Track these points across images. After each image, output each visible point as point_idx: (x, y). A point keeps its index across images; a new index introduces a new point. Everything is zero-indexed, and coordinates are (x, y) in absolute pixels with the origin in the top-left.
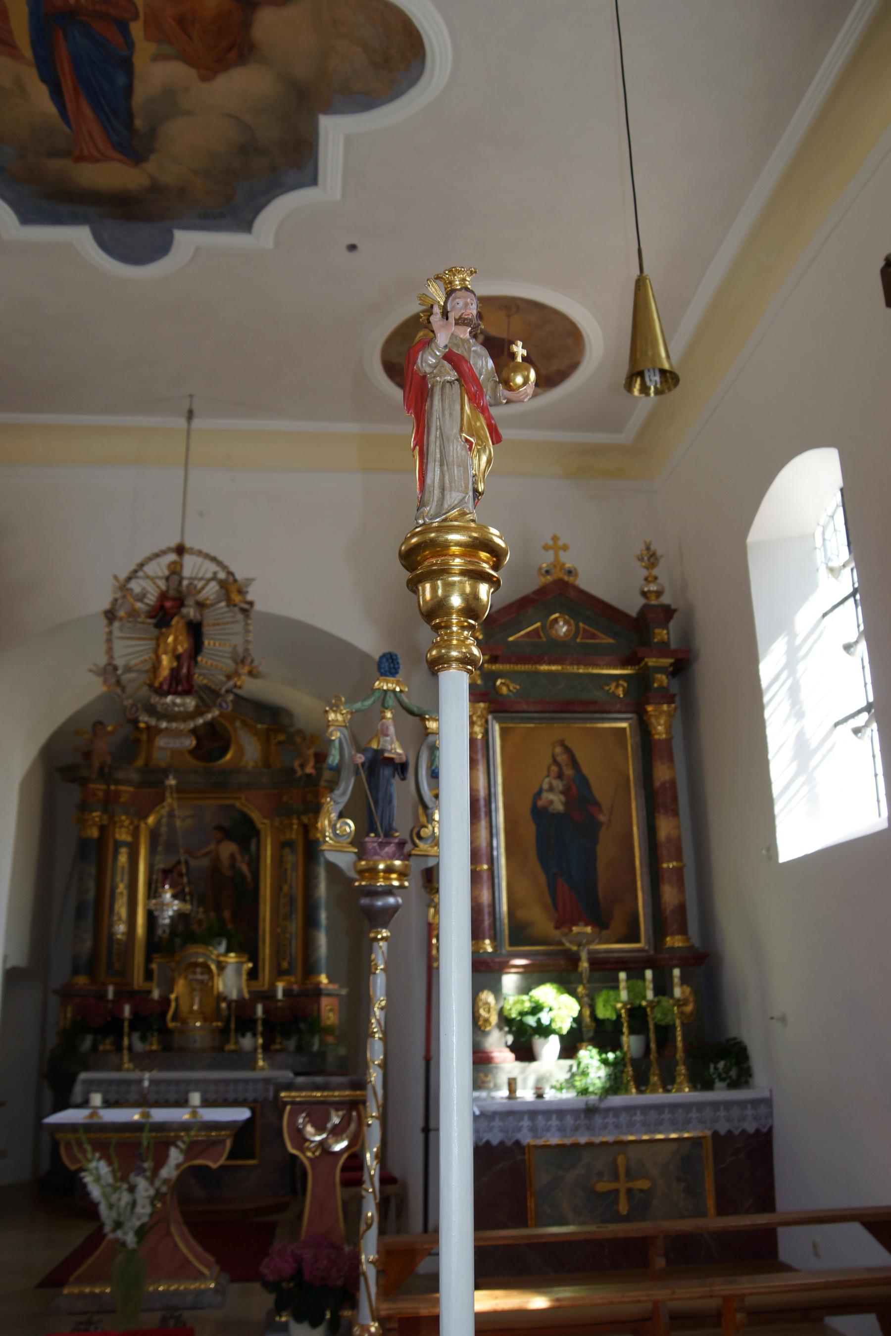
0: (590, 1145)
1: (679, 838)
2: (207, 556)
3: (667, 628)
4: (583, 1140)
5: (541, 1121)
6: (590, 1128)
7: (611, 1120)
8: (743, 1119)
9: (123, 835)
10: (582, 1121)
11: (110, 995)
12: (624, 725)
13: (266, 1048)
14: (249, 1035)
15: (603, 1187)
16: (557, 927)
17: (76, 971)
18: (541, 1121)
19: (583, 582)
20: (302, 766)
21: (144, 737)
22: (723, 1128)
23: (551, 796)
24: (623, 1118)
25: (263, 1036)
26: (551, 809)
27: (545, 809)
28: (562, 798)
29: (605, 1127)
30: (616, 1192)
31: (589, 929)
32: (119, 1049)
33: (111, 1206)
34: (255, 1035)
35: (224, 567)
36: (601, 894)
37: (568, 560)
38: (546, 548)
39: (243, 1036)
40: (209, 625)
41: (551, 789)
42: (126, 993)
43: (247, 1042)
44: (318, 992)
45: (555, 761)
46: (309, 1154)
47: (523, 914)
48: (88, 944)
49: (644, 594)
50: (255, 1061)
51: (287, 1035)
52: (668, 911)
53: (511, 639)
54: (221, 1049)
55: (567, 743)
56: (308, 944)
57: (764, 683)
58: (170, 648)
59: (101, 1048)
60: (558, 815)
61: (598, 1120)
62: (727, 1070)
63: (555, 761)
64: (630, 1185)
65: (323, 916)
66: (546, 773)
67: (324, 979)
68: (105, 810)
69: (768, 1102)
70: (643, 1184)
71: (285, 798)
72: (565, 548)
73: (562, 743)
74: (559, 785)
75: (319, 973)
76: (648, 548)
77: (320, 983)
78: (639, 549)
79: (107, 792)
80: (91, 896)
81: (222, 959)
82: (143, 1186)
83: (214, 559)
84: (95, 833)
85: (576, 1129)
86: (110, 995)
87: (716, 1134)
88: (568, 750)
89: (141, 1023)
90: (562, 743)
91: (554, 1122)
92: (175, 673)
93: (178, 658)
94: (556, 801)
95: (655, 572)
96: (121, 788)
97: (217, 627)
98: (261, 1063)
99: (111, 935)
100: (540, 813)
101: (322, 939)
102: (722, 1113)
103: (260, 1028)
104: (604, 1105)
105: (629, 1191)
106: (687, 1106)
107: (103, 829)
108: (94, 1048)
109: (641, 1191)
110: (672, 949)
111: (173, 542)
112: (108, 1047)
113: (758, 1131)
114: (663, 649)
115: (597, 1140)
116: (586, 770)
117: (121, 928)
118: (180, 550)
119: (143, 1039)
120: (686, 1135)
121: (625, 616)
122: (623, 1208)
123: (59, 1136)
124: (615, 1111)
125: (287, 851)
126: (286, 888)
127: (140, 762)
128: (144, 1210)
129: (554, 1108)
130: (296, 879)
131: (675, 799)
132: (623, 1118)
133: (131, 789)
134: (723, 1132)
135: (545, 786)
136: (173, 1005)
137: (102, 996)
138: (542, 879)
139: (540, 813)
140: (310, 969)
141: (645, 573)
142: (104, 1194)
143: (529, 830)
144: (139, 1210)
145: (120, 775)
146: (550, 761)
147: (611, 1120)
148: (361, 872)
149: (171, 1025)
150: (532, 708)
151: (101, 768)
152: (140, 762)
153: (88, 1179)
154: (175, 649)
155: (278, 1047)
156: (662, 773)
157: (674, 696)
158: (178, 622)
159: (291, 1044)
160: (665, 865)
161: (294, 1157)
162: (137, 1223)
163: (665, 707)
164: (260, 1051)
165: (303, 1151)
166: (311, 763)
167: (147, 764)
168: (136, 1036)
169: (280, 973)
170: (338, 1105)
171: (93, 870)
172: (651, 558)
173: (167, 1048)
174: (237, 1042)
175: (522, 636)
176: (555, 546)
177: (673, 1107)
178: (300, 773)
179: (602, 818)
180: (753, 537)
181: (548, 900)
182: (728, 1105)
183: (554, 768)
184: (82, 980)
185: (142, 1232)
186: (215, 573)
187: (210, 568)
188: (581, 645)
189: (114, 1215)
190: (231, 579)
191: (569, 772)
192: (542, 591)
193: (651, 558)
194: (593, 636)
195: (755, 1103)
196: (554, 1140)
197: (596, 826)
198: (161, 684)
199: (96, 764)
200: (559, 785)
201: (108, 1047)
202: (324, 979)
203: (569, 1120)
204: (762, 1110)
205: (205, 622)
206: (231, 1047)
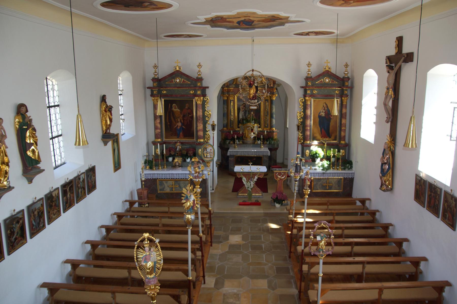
0: (323, 179)
1: (346, 123)
2: (258, 71)
3: (348, 82)
4: (322, 178)
5: (315, 174)
6: (323, 176)
7: (327, 175)
8: (349, 176)
9: (231, 98)
10: (322, 175)
11: (232, 133)
12: (338, 99)
13: (263, 143)
14: (260, 141)
15: (324, 185)
16: (321, 138)
17: (224, 127)
18: (315, 174)
19: (333, 71)
20: (270, 85)
22: (345, 177)
23: (322, 113)
24: (329, 175)
25: (262, 142)
26: (322, 116)
27: (321, 116)
28: (324, 114)
29: (326, 176)
30: (327, 186)
31: (327, 139)
32: (234, 143)
33: (247, 185)
34: (261, 141)
35: (261, 74)
36: (330, 132)
37: (329, 65)
38: (325, 63)
39: (258, 141)
41: (322, 112)
42: (235, 132)
43: (259, 142)
44: (273, 132)
45: (323, 106)
46: (278, 180)
47: (315, 135)
48: (226, 121)
49: (344, 73)
50: (261, 146)
51: (267, 141)
52: (342, 137)
53: (317, 83)
54: (254, 143)
55: (326, 103)
56: (271, 121)
57: (363, 104)
59: (231, 143)
60: (323, 117)
61: (325, 175)
62: (348, 166)
63: (323, 106)
64: (329, 185)
65: (274, 116)
66: (321, 109)
67: (274, 129)
68: (228, 94)
69: (354, 173)
70: (331, 185)
72: (329, 63)
73: (325, 103)
74: (324, 111)
75: (273, 128)
76: (346, 64)
77: (274, 130)
78: (344, 64)
79: (228, 89)
80: (226, 112)
81: (254, 125)
82: (252, 182)
83: (259, 72)
84: (226, 98)
85: (321, 176)
86: (232, 133)
87: (344, 178)
88: (326, 104)
89: (238, 138)
90: (325, 103)
91: (317, 175)
92: (253, 97)
93: (254, 94)
94: (323, 114)
95: (347, 69)
96: (230, 88)
98: (262, 147)
99: (230, 120)
100: (320, 117)
101: (274, 121)
102: (346, 175)
103: (262, 140)
104: (326, 172)
105: (329, 186)
106: (340, 173)
107: (227, 97)
108: (229, 143)
109: (331, 186)
110: (342, 144)
111: (251, 69)
112: (232, 143)
113: (351, 178)
114: (347, 87)
115: (324, 178)
116: (329, 109)
117: (232, 117)
118: (253, 70)
119: (239, 141)
120: (339, 178)
121: (340, 78)
122: (327, 188)
123: (237, 173)
124: (328, 173)
125: (267, 101)
126: (266, 110)
127: (235, 83)
128: (252, 186)
129: (318, 172)
130: (268, 108)
131: (346, 116)
132: (329, 175)
133: (233, 88)
134: (345, 177)
135: (321, 111)
136: (244, 135)
137: (230, 132)
138: (319, 129)
139: (320, 117)
140: (271, 127)
141: (345, 69)
142: (246, 184)
143: (318, 120)
144: (251, 186)
145: (231, 86)
146: (323, 106)
147: (327, 175)
148: (295, 177)
149: (244, 138)
150: (320, 96)
152: (235, 83)
153: (243, 181)
154: (253, 92)
155: (265, 143)
156: (344, 111)
157: (348, 95)
159: (268, 143)
160: (342, 128)
161: (276, 180)
162: (251, 188)
163: (346, 98)
164: (262, 144)
165: (277, 179)
167: (236, 83)
168: (237, 141)
169: (265, 127)
170: (283, 173)
171: (226, 106)
172: (346, 66)
173: (243, 143)
174: (257, 142)
175: (319, 82)
176: (327, 62)
177: (337, 173)
178: (270, 86)
179: (332, 117)
180: (365, 75)
181: (320, 132)
182: (347, 173)
183: (323, 108)
184: (225, 129)
185: (252, 189)
187: (259, 74)
188: (331, 84)
189: (248, 186)
191: (326, 109)
192: (324, 73)
193: (346, 66)
194: (333, 82)
195: (352, 173)
196: (317, 177)
197: (331, 119)
200: (324, 111)
201: (232, 143)
202: (274, 129)
203: (320, 175)
204: (353, 174)
206: (256, 143)
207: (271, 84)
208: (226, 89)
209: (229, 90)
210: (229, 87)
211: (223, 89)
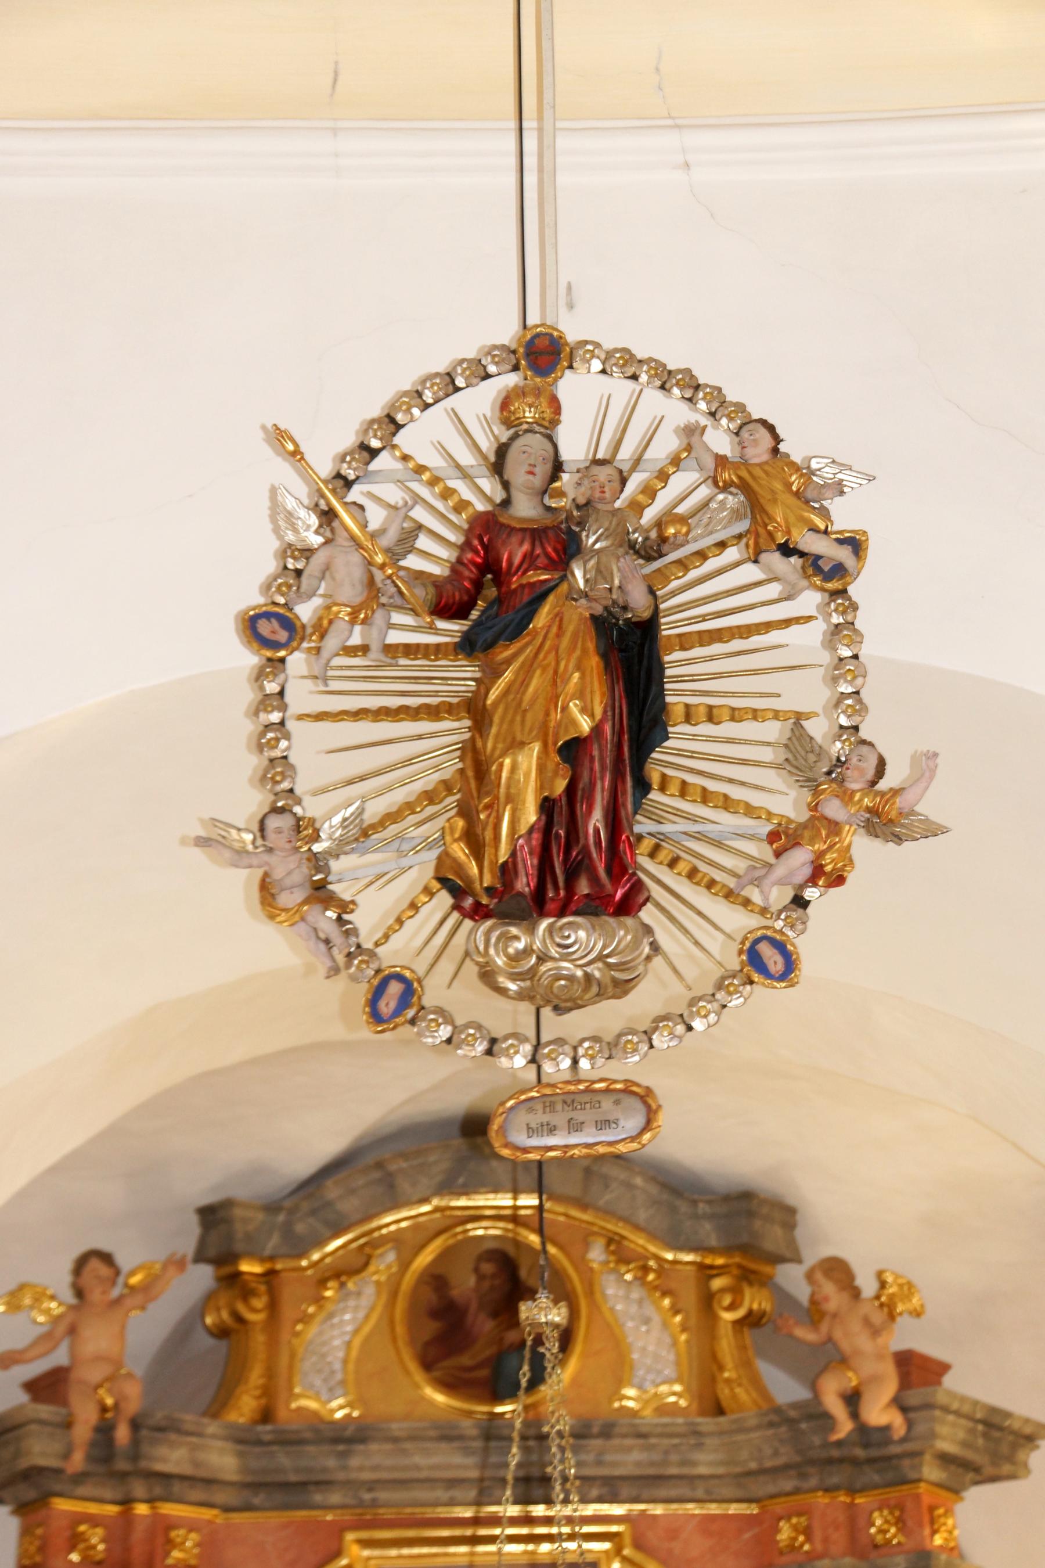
20: (853, 1399)
21: (255, 1314)
40: (684, 642)
58: (534, 717)
71: (785, 1533)
97: (717, 648)
151: (105, 1430)
158: (558, 618)
166: (890, 1387)
167: (266, 1416)
178: (845, 1427)
186: (691, 432)
190: (759, 451)
198: (507, 871)
199: (86, 1417)
205: (668, 629)
207: (875, 1379)
208: (93, 1521)
209: (139, 1533)
210: (135, 1453)
211: (26, 1532)
